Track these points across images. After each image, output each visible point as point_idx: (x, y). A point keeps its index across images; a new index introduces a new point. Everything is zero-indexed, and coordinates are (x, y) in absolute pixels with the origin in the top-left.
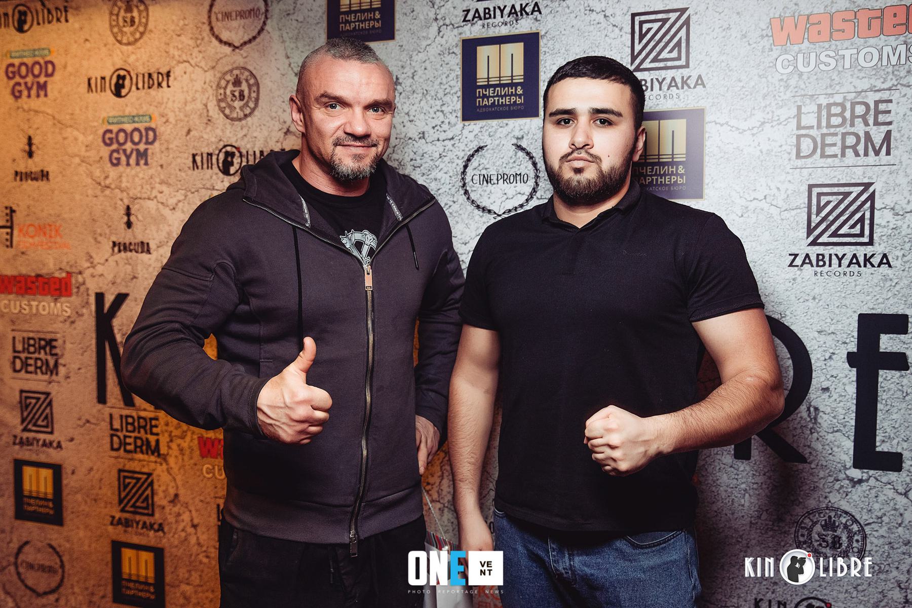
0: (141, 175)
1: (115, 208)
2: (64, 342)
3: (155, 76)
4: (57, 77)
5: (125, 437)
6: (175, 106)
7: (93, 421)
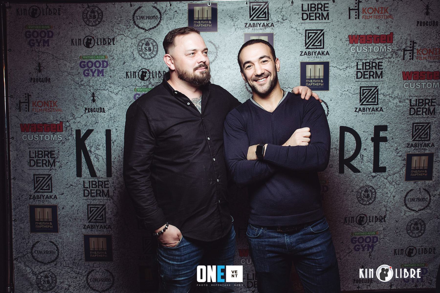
0: (100, 80)
1: (87, 94)
2: (59, 152)
4: (55, 38)
5: (91, 190)
6: (117, 52)
7: (73, 185)
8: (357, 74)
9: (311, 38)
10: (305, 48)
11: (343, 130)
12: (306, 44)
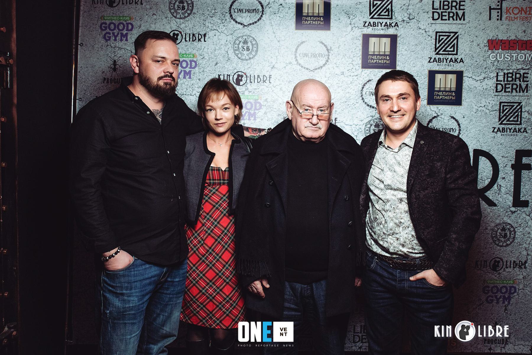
0: (186, 83)
3: (197, 36)
8: (496, 87)
9: (442, 41)
10: (434, 53)
11: (478, 153)
12: (436, 49)
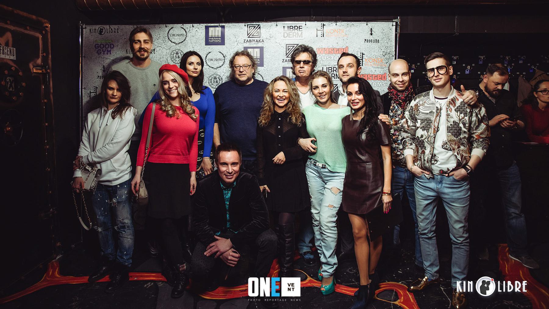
4: (115, 48)
